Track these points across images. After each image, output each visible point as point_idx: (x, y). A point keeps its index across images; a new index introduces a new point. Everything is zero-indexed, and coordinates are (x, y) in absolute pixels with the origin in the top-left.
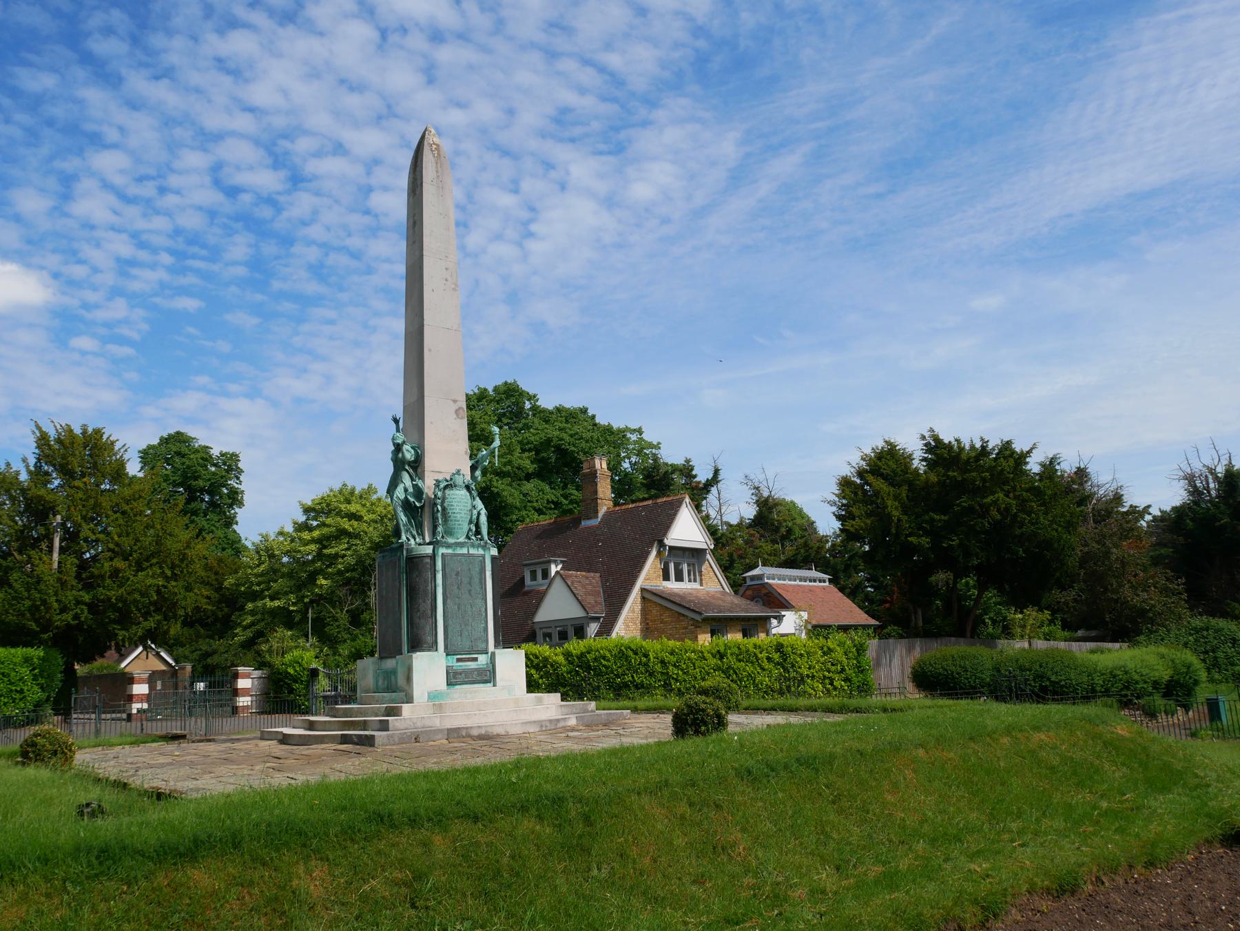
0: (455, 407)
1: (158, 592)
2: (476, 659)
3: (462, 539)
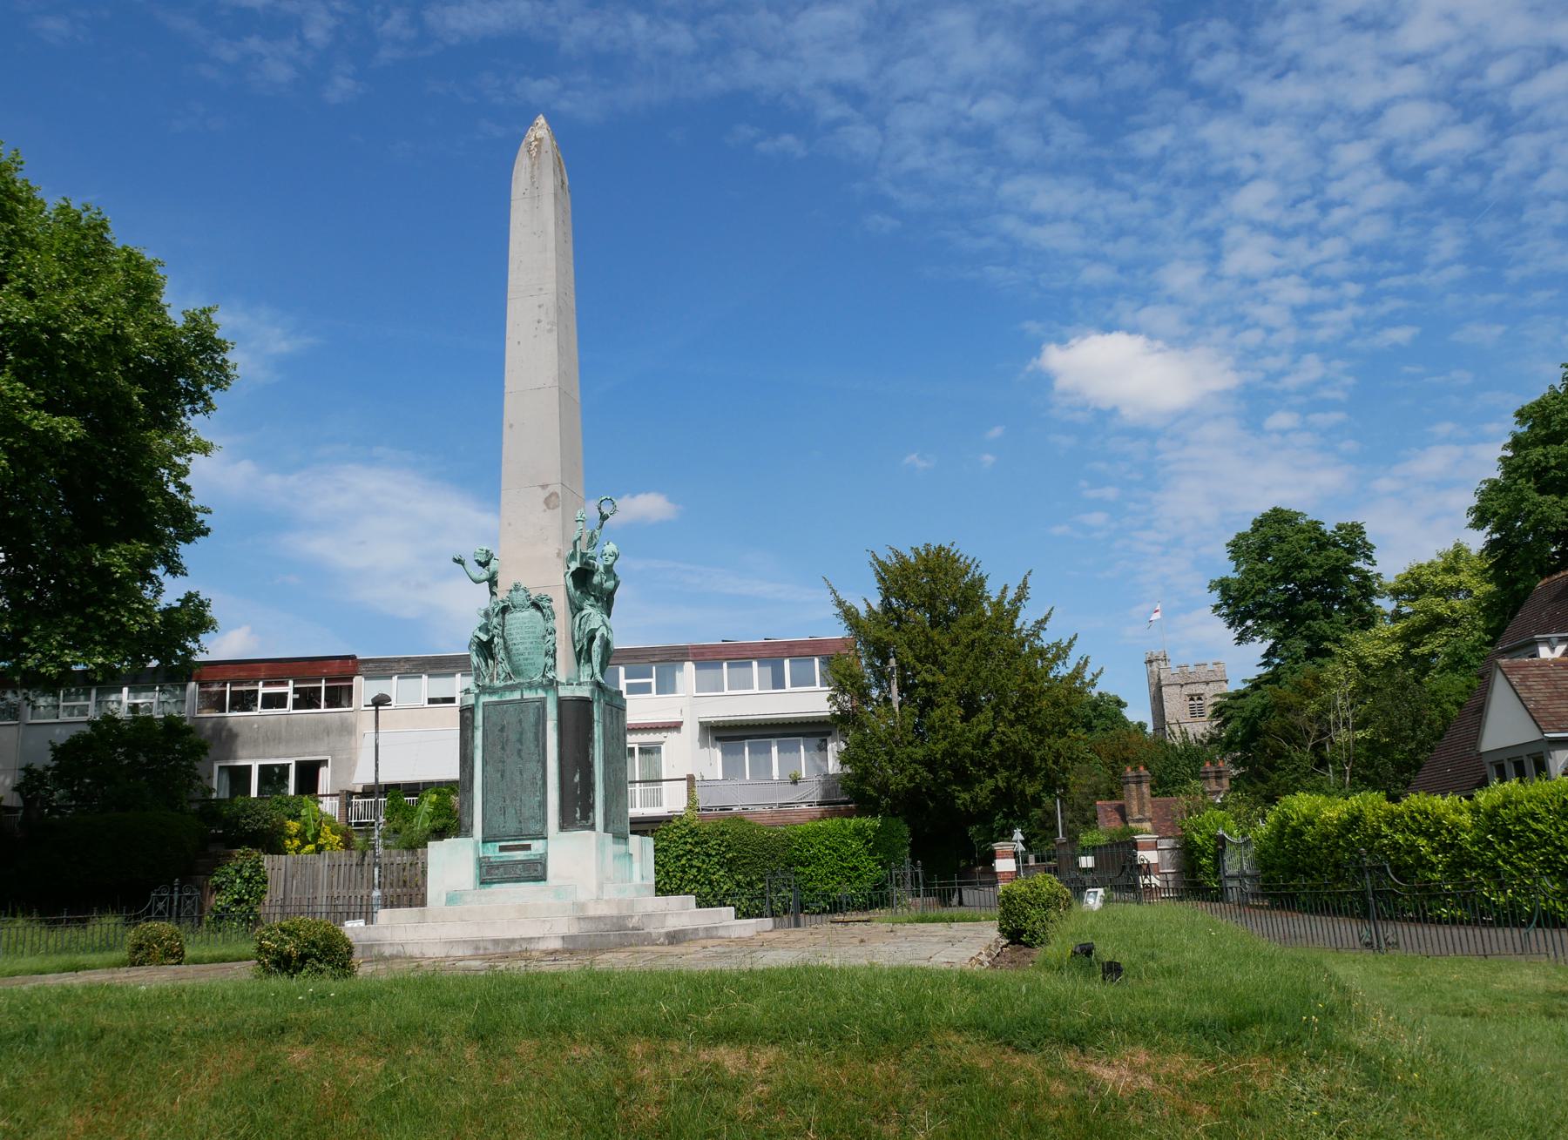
0: (546, 493)
1: (1001, 742)
2: (528, 847)
3: (538, 678)
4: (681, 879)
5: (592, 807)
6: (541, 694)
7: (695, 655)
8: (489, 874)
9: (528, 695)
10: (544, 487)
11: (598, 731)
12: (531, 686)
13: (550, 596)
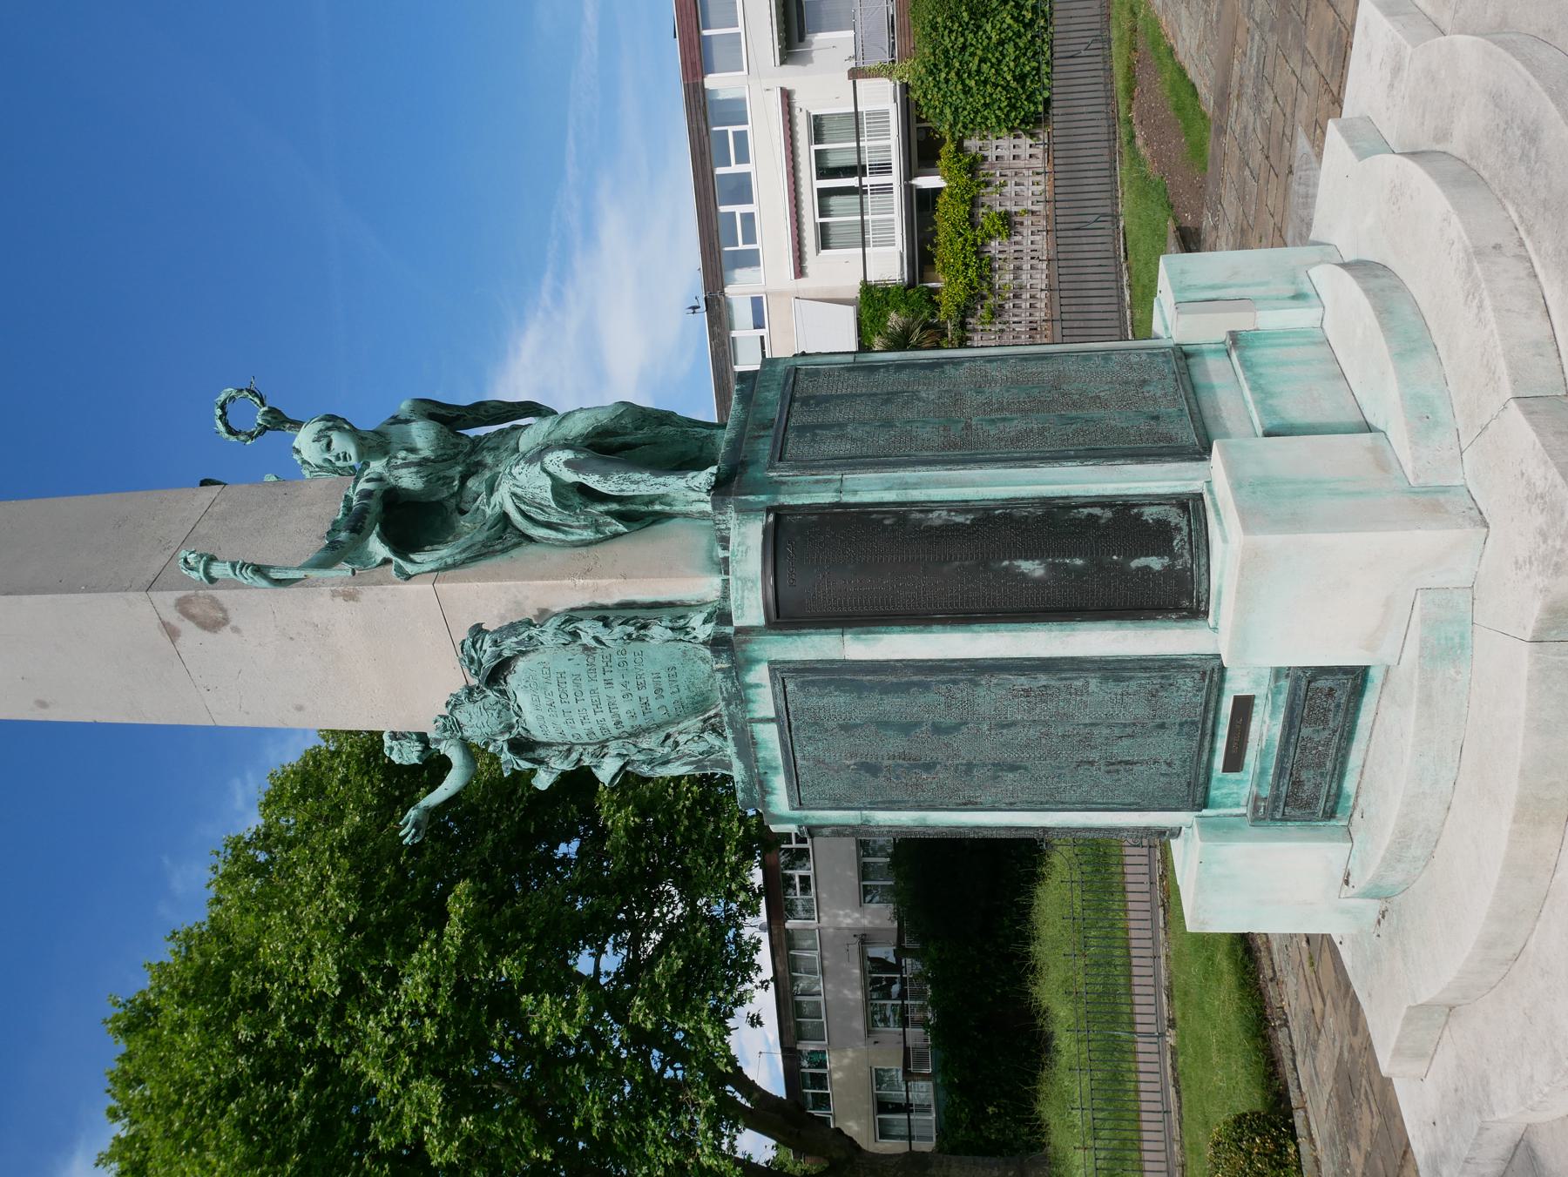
2: (1244, 706)
4: (996, 85)
5: (1124, 508)
7: (695, 75)
8: (1308, 791)
9: (764, 703)
10: (173, 633)
11: (870, 488)
12: (740, 697)
13: (463, 634)
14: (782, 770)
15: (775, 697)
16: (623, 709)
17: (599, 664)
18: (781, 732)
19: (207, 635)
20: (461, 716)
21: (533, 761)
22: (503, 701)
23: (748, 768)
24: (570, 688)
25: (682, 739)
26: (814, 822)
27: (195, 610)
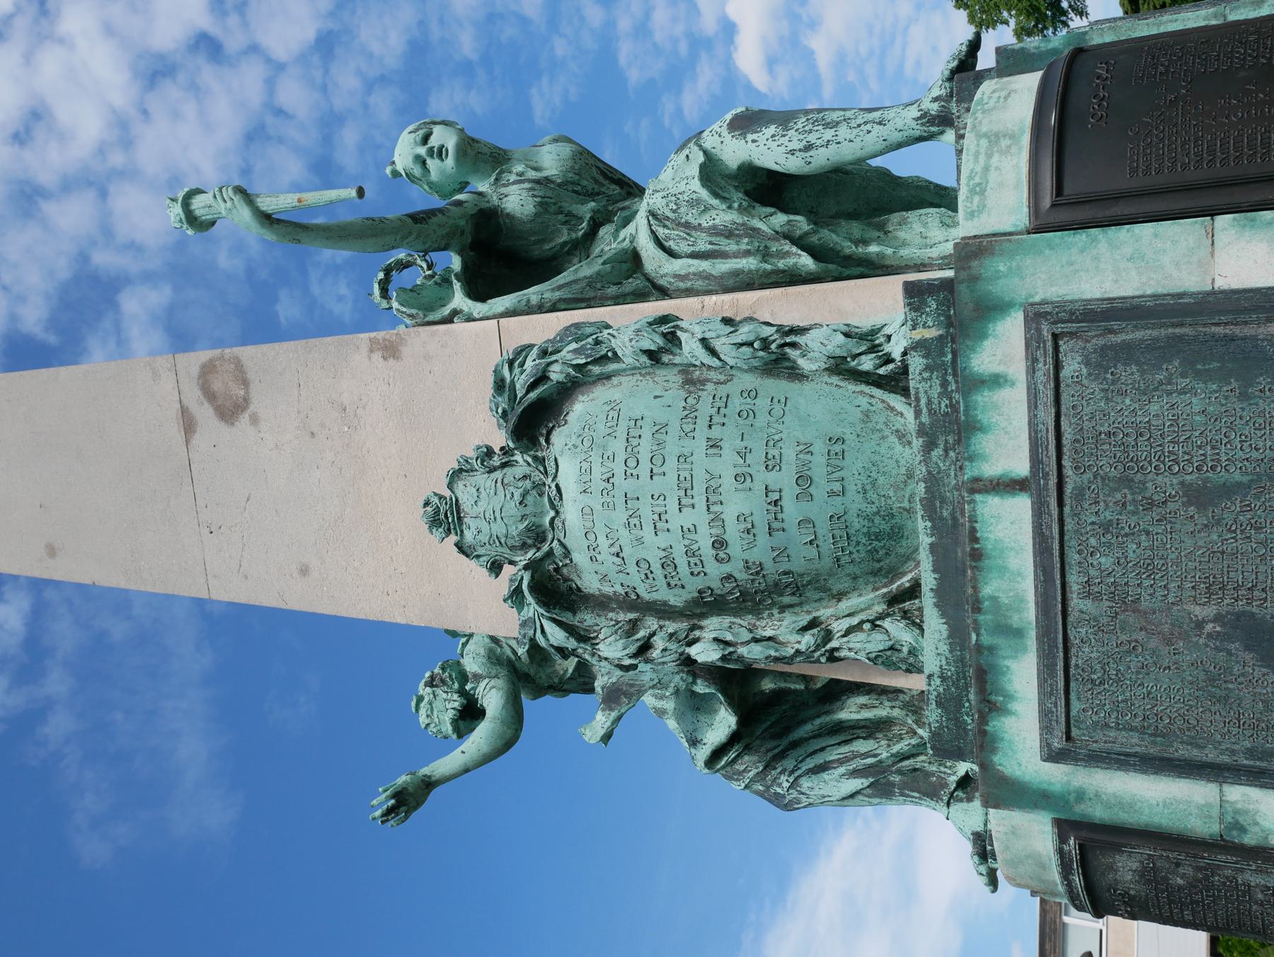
6: (1003, 349)
14: (1031, 641)
15: (1033, 404)
16: (735, 505)
17: (705, 408)
18: (1039, 511)
19: (222, 428)
20: (465, 493)
21: (570, 630)
22: (538, 477)
23: (957, 635)
24: (645, 448)
25: (839, 626)
26: (1098, 813)
27: (217, 385)
